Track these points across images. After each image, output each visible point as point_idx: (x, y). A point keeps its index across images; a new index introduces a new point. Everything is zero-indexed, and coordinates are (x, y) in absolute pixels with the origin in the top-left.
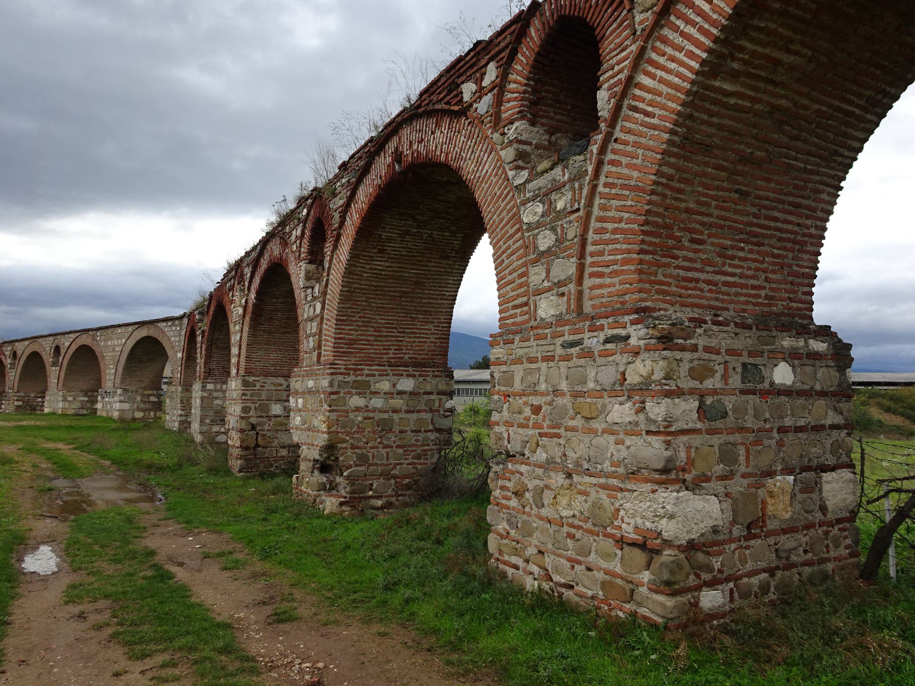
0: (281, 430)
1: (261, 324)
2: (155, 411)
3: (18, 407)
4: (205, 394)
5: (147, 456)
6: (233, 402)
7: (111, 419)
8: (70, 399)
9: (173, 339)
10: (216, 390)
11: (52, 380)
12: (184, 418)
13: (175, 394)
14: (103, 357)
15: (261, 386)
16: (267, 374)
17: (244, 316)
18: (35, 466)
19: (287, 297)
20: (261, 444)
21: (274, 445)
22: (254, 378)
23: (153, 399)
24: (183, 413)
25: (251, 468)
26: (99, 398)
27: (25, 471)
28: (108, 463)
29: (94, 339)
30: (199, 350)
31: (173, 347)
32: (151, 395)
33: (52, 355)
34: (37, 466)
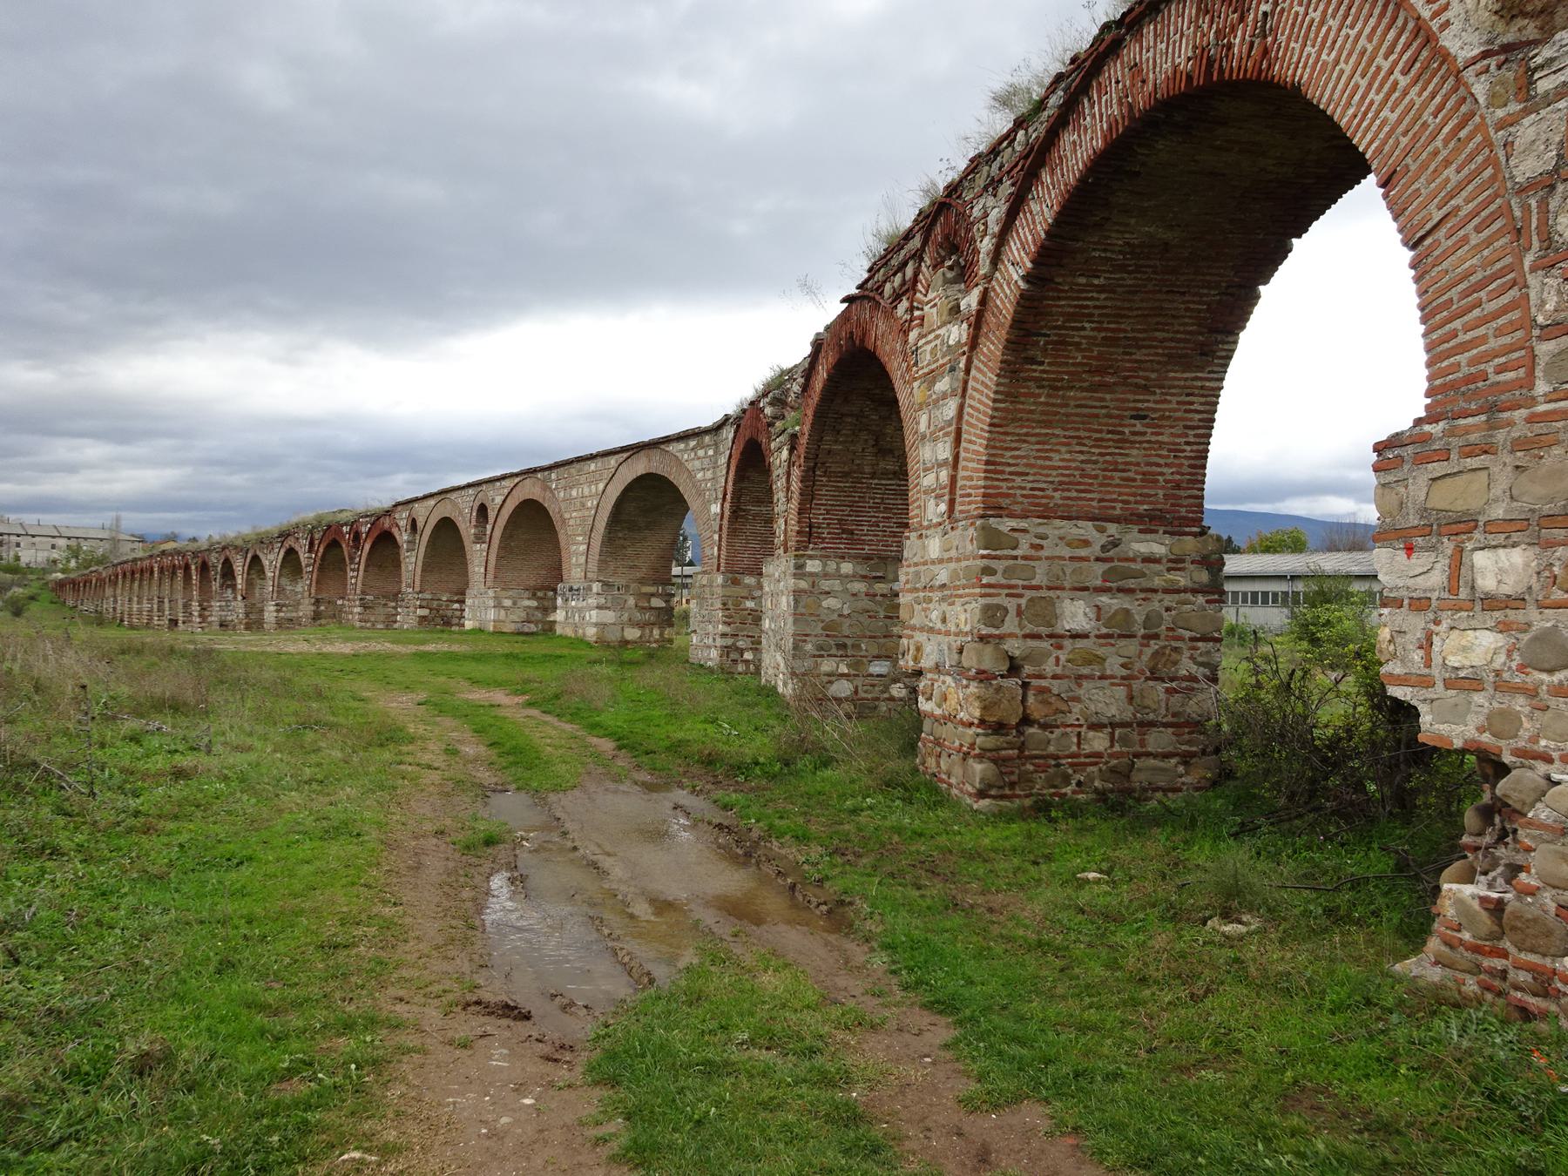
0: (1086, 677)
1: (1033, 361)
2: (662, 628)
3: (423, 618)
4: (803, 584)
5: (692, 731)
6: (936, 595)
7: (581, 641)
8: (508, 603)
9: (699, 476)
10: (826, 576)
11: (476, 569)
12: (729, 641)
13: (707, 590)
14: (564, 521)
15: (1033, 546)
16: (1046, 514)
17: (974, 343)
18: (451, 752)
19: (1122, 268)
20: (1036, 715)
21: (1071, 719)
22: (1013, 523)
23: (657, 603)
24: (727, 629)
25: (1012, 785)
26: (559, 601)
27: (430, 767)
28: (607, 745)
29: (546, 488)
30: (780, 484)
31: (700, 493)
32: (653, 595)
33: (474, 523)
34: (455, 753)
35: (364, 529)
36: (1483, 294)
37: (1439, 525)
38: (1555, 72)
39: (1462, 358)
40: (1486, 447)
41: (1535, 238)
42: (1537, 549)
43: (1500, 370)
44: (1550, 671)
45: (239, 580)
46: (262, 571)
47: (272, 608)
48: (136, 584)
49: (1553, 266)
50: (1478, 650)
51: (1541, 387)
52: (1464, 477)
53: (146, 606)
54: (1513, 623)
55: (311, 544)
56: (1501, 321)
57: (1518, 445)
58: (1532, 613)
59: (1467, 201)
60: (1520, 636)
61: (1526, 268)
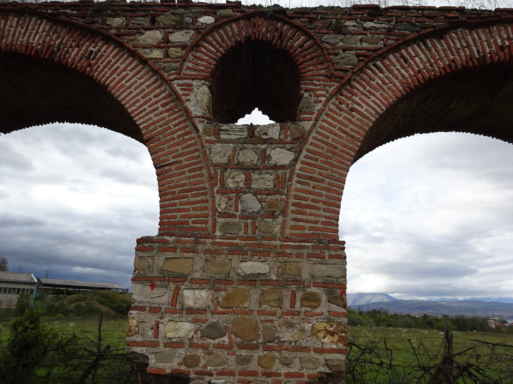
36: (189, 194)
37: (169, 278)
38: (227, 134)
39: (178, 215)
40: (194, 250)
41: (219, 183)
42: (213, 292)
43: (194, 222)
44: (214, 339)
49: (224, 194)
50: (183, 330)
51: (218, 233)
52: (182, 260)
54: (199, 319)
56: (196, 205)
57: (206, 252)
58: (209, 316)
59: (186, 160)
60: (202, 325)
61: (215, 191)
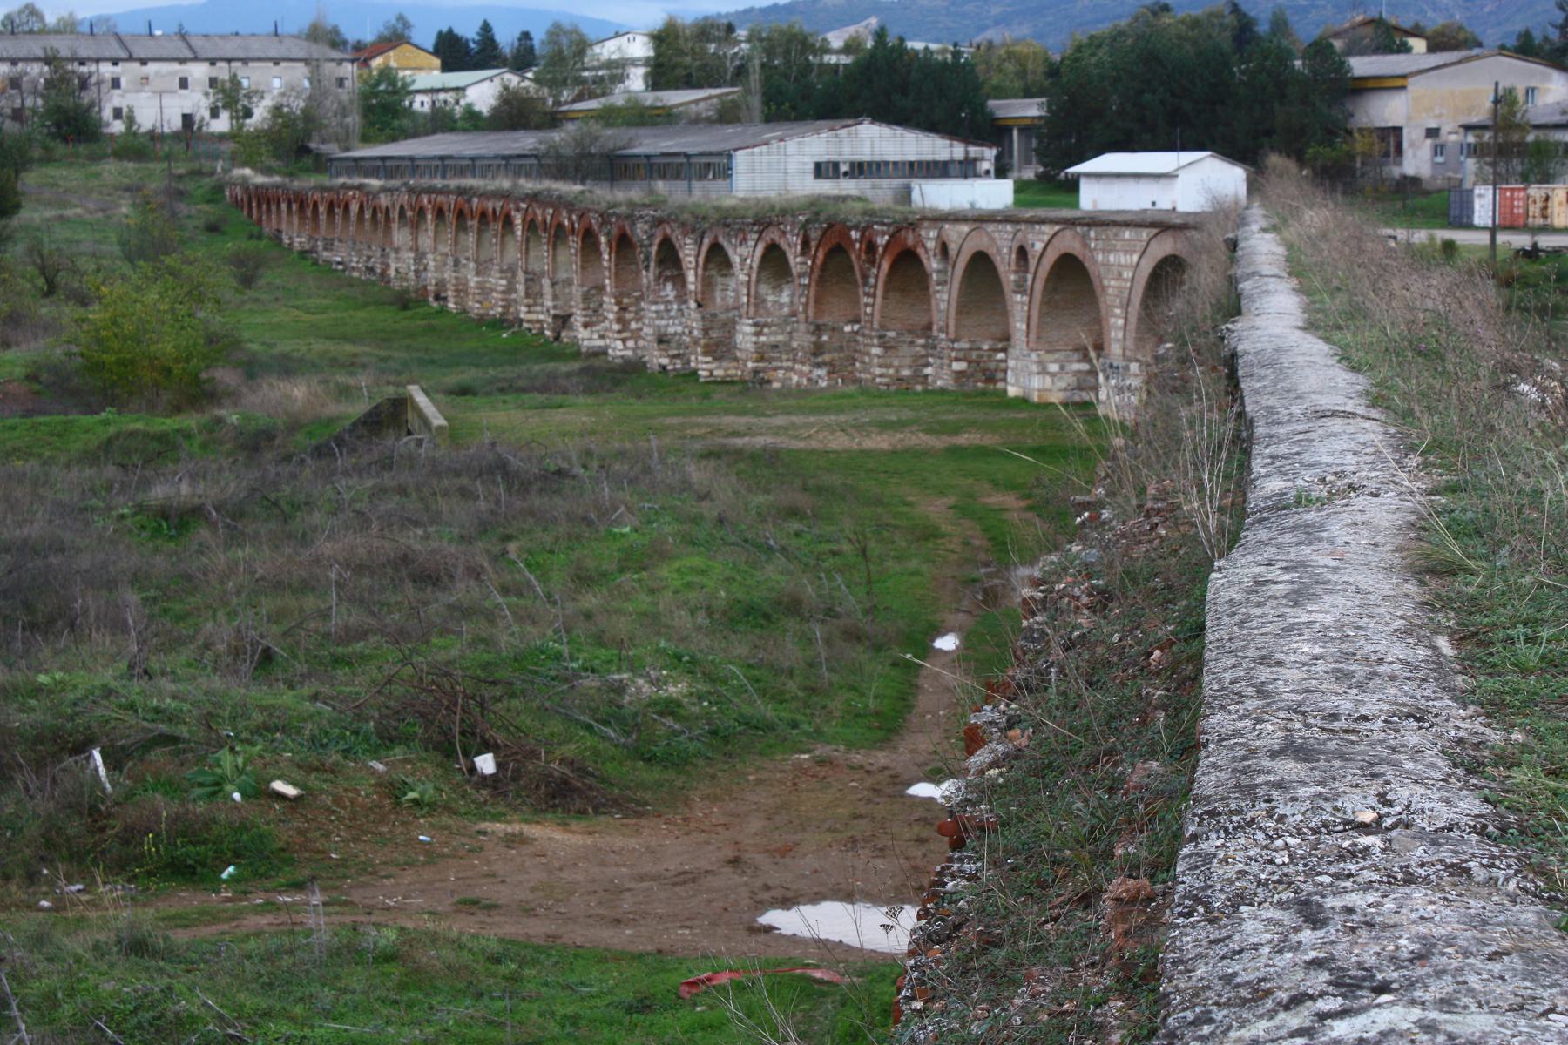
8: (1054, 368)
14: (1104, 288)
18: (966, 544)
27: (953, 552)
33: (1013, 267)
34: (968, 544)
35: (882, 241)
45: (691, 277)
46: (727, 264)
47: (749, 329)
48: (471, 239)
53: (498, 282)
55: (806, 244)
